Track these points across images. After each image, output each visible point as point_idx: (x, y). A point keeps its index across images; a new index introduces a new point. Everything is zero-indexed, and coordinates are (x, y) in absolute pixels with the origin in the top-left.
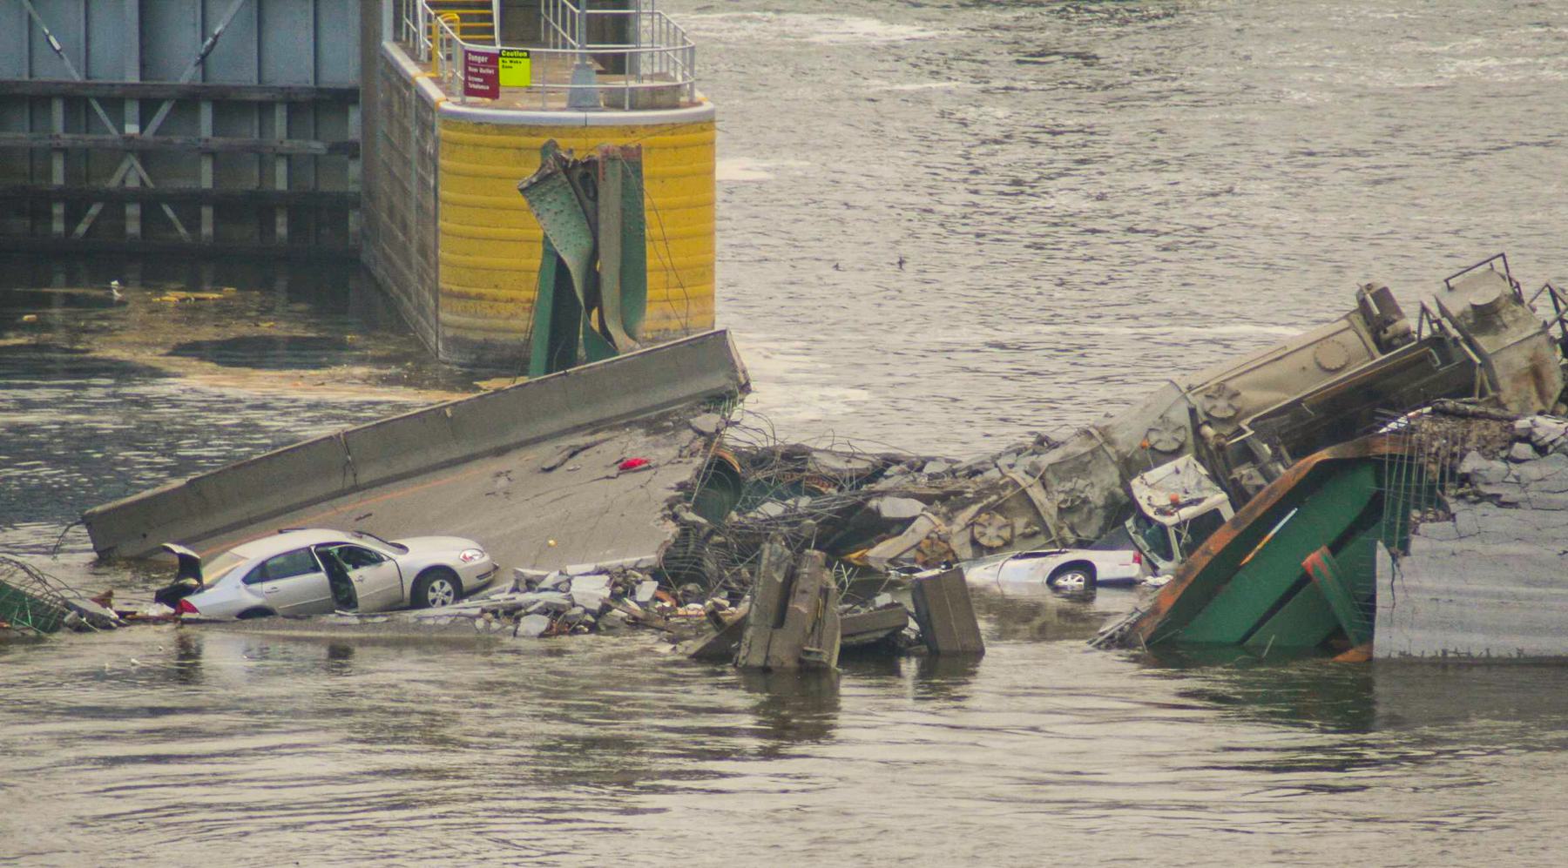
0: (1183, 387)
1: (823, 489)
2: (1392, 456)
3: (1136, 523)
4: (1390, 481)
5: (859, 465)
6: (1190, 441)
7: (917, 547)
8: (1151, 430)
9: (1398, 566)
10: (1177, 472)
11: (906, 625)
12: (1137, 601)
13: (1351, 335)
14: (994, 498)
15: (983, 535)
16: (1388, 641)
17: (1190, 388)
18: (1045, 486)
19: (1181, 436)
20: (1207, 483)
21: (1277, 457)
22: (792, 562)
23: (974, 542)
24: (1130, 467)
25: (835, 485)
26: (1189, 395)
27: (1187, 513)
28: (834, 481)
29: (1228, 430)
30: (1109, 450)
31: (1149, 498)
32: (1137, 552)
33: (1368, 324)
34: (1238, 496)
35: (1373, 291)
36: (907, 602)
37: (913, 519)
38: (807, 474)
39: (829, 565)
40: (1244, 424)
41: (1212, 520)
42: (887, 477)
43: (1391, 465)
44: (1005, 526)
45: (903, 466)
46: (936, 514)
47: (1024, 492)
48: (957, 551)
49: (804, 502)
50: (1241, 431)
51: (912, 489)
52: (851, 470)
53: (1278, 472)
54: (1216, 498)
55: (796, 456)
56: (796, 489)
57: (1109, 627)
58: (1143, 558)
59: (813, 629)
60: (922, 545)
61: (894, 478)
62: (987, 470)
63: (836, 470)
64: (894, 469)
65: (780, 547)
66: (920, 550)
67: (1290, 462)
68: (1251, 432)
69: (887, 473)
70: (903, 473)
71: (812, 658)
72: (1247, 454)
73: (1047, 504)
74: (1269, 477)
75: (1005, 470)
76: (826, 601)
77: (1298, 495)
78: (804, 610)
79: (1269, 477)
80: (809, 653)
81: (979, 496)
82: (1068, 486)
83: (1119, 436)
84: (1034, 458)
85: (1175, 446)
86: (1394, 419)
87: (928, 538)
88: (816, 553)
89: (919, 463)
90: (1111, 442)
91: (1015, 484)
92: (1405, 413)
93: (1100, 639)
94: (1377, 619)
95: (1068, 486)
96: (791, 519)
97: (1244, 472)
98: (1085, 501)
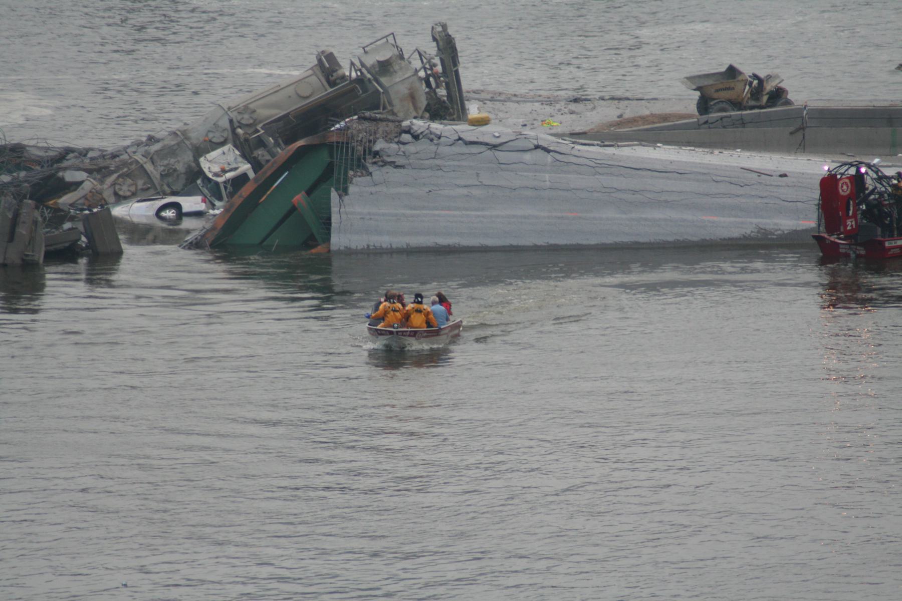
0: (226, 107)
1: (33, 167)
2: (338, 143)
3: (203, 181)
4: (337, 155)
5: (51, 154)
6: (230, 136)
7: (85, 197)
8: (209, 131)
9: (342, 201)
10: (224, 153)
11: (80, 239)
12: (204, 223)
13: (314, 78)
14: (126, 170)
15: (121, 189)
16: (338, 240)
17: (229, 108)
18: (153, 163)
19: (225, 134)
20: (240, 159)
21: (277, 144)
22: (17, 207)
23: (116, 194)
24: (200, 151)
25: (40, 164)
26: (229, 112)
27: (229, 175)
28: (39, 162)
29: (250, 131)
30: (187, 142)
31: (209, 168)
32: (204, 198)
33: (323, 72)
34: (257, 165)
35: (325, 55)
36: (80, 227)
37: (82, 182)
38: (24, 159)
39: (37, 208)
40: (259, 127)
41: (242, 179)
42: (67, 160)
43: (337, 147)
44: (132, 185)
45: (76, 154)
46: (94, 179)
47: (142, 166)
48: (107, 198)
49: (23, 174)
50: (258, 131)
51: (81, 166)
52: (47, 156)
53: (278, 152)
54: (245, 167)
55: (17, 149)
56: (18, 167)
57: (189, 238)
58: (207, 201)
59: (29, 244)
60: (88, 196)
61: (71, 160)
62: (122, 155)
63: (39, 156)
64: (71, 155)
65: (10, 198)
66: (86, 199)
67: (284, 147)
68: (262, 132)
69: (68, 157)
70: (76, 157)
72: (261, 143)
73: (155, 172)
74: (273, 155)
75: (131, 155)
76: (36, 227)
77: (288, 165)
78: (24, 233)
79: (273, 155)
80: (27, 255)
81: (118, 169)
82: (166, 162)
83: (192, 135)
84: (146, 148)
85: (222, 140)
86: (338, 122)
87: (90, 192)
88: (30, 201)
89: (85, 152)
90: (188, 138)
91: (137, 162)
92: (344, 119)
93: (185, 244)
94: (332, 230)
95: (166, 162)
96: (16, 183)
97: (260, 153)
98: (175, 170)
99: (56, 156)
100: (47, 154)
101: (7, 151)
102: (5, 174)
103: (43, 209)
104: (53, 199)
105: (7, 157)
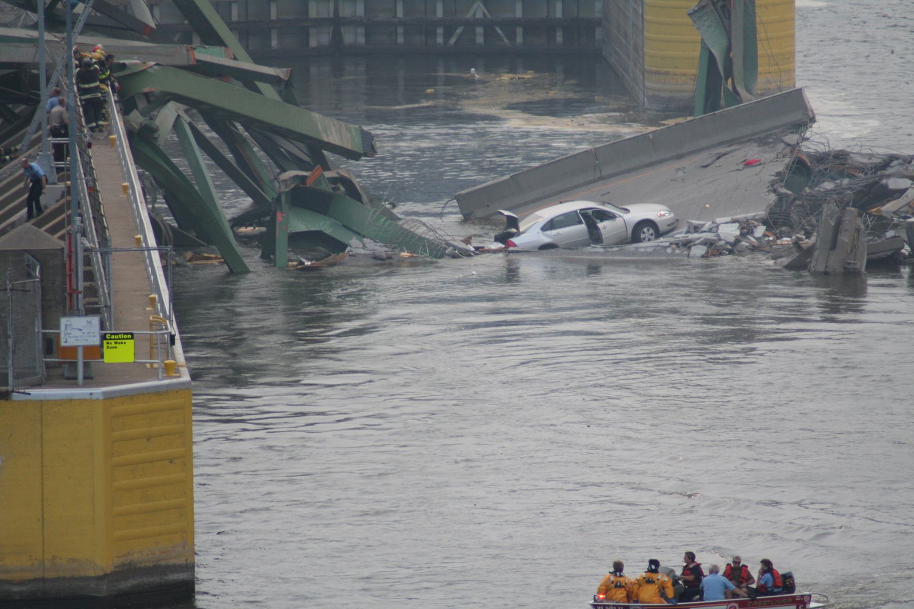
1: (856, 174)
5: (875, 160)
7: (908, 204)
22: (840, 215)
25: (863, 172)
28: (863, 169)
36: (904, 236)
37: (906, 190)
38: (847, 166)
39: (860, 215)
42: (892, 167)
45: (900, 161)
49: (846, 181)
51: (906, 173)
52: (871, 163)
56: (842, 174)
59: (851, 251)
60: (911, 204)
61: (895, 167)
63: (863, 163)
64: (895, 162)
65: (833, 206)
66: (910, 207)
69: (892, 164)
70: (900, 164)
71: (851, 266)
76: (859, 234)
78: (847, 240)
80: (849, 264)
88: (853, 209)
89: (909, 159)
96: (839, 191)
99: (880, 163)
100: (871, 161)
101: (831, 158)
102: (828, 181)
103: (866, 217)
104: (876, 207)
105: (830, 164)
